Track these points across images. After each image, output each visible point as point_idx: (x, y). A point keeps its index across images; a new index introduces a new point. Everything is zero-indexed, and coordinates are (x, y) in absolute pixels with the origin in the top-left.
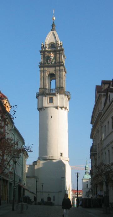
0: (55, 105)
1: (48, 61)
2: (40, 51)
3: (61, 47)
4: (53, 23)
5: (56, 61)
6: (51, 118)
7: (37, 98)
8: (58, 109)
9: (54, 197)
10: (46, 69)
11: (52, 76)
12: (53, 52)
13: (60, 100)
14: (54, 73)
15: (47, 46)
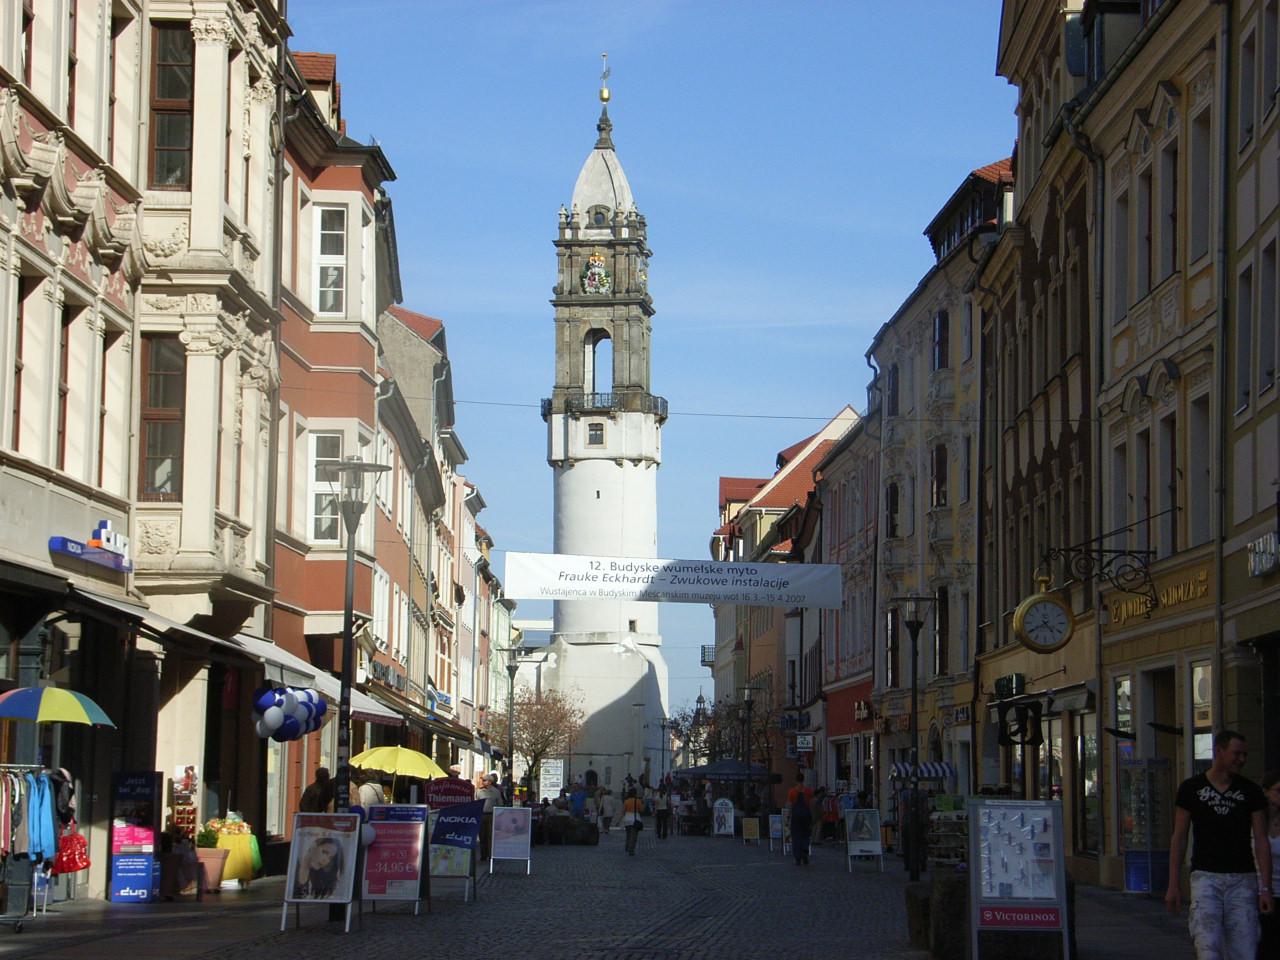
1: (586, 281)
4: (604, 113)
6: (598, 497)
7: (546, 420)
8: (620, 465)
9: (608, 770)
10: (578, 311)
13: (631, 431)
15: (583, 220)
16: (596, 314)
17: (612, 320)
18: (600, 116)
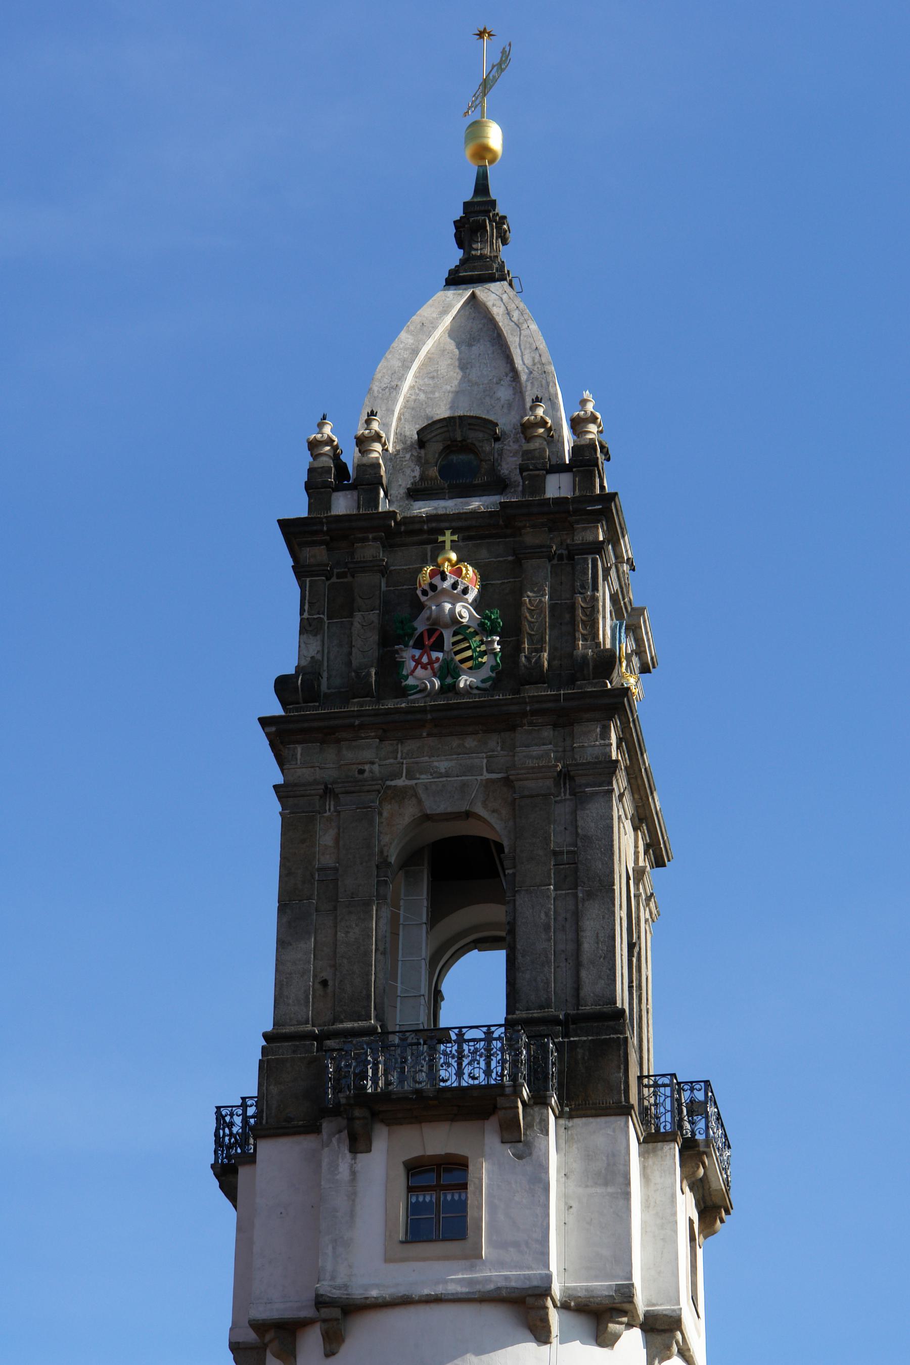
0: (495, 1268)
2: (284, 524)
3: (586, 460)
4: (482, 186)
5: (511, 650)
7: (230, 1189)
10: (368, 756)
11: (464, 876)
12: (473, 534)
14: (494, 823)
16: (443, 765)
17: (507, 782)
18: (468, 195)
